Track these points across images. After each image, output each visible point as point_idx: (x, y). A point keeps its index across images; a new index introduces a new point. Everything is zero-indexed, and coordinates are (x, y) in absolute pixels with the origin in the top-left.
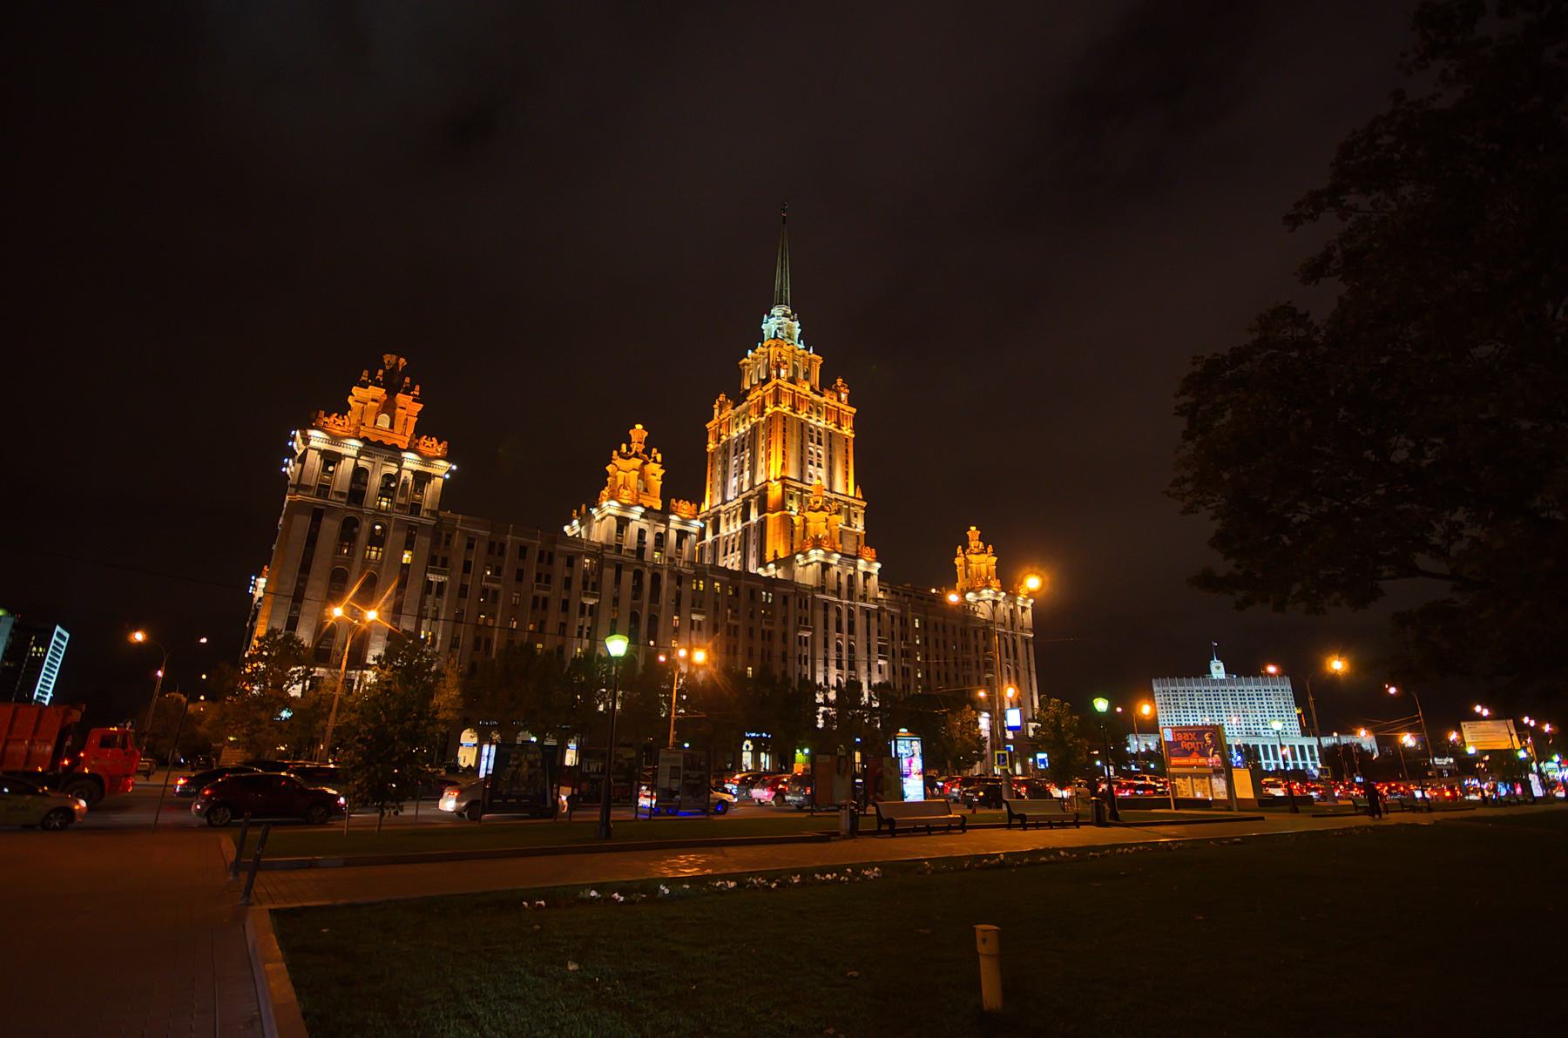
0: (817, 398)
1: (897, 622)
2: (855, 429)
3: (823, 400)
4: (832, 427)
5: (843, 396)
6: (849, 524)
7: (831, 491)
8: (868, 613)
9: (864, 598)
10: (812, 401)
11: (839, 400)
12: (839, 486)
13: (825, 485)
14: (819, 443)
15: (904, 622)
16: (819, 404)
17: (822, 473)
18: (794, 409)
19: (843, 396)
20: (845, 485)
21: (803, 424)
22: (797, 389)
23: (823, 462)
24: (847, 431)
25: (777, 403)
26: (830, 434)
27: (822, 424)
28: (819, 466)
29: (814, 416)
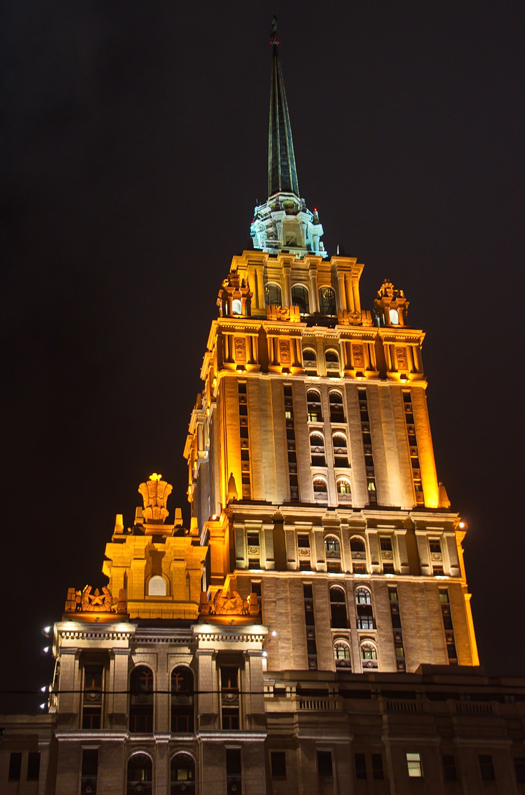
0: (320, 331)
1: (342, 769)
2: (425, 370)
3: (337, 331)
4: (366, 379)
5: (394, 316)
6: (415, 567)
7: (373, 504)
8: (234, 759)
9: (231, 720)
10: (312, 341)
11: (386, 324)
12: (396, 492)
13: (357, 500)
14: (337, 416)
15: (372, 767)
16: (327, 343)
17: (349, 476)
18: (264, 364)
19: (394, 316)
20: (411, 485)
21: (288, 392)
22: (267, 326)
23: (350, 453)
24: (406, 378)
25: (223, 362)
26: (363, 396)
27: (340, 381)
28: (341, 463)
29: (321, 368)
